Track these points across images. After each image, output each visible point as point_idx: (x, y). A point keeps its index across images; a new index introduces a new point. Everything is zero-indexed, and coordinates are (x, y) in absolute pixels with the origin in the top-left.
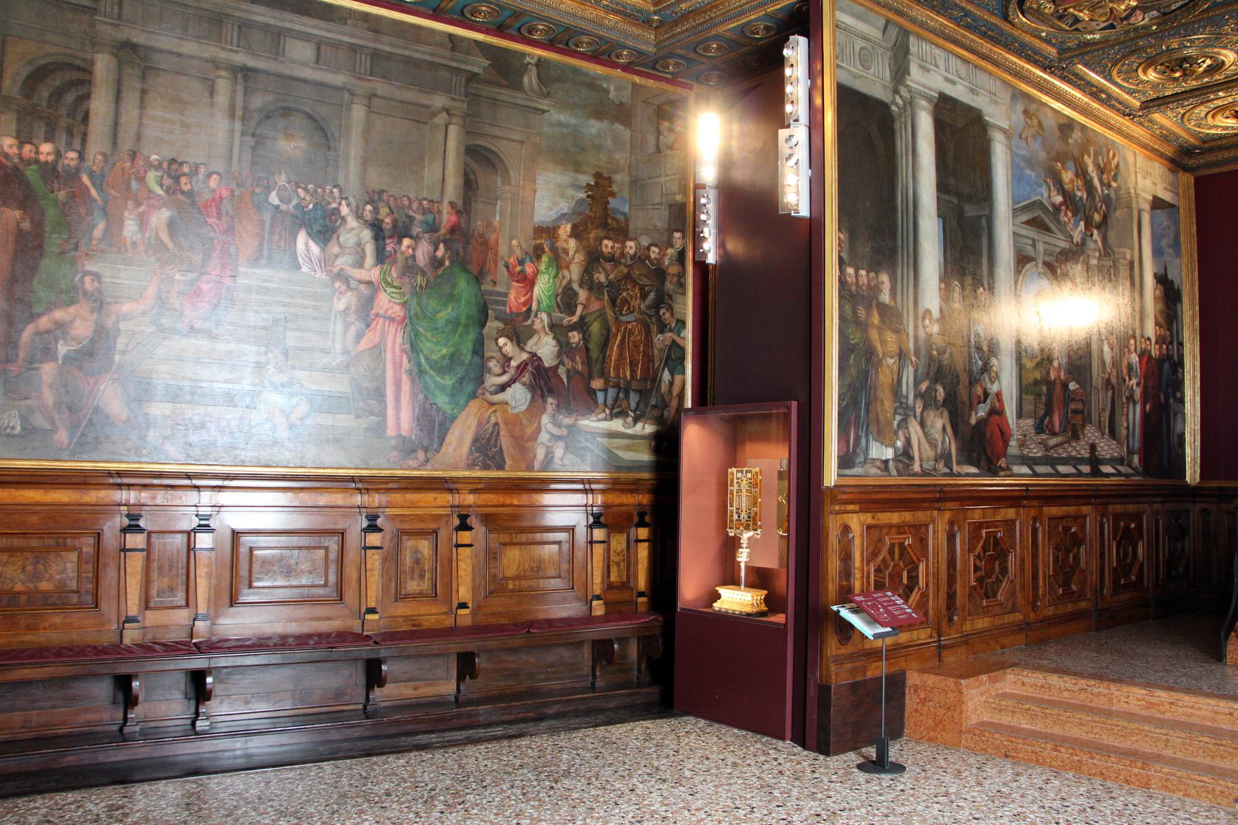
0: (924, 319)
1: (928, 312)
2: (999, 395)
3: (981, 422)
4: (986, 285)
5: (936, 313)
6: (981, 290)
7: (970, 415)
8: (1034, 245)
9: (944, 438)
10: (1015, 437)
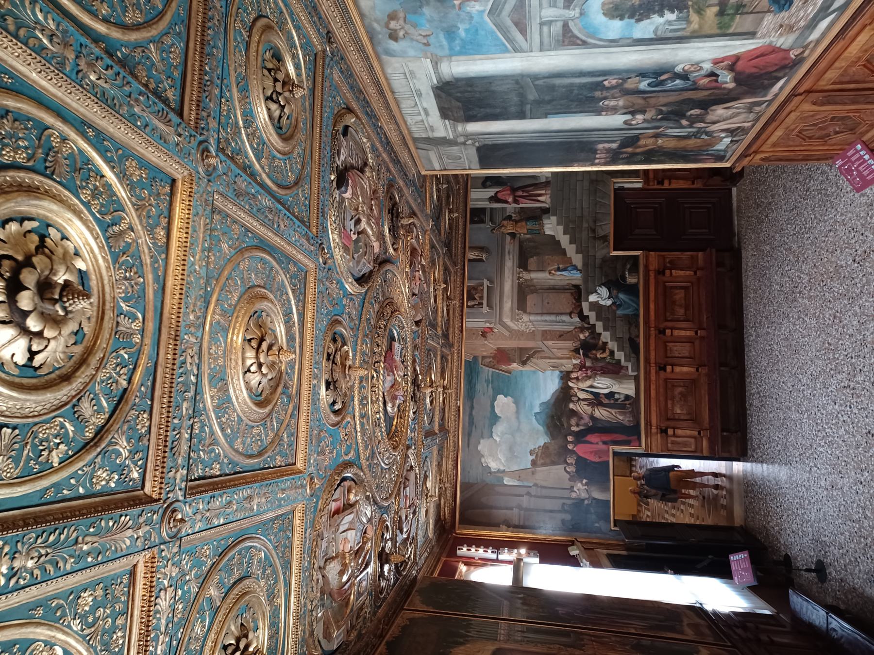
0: (631, 125)
1: (625, 122)
2: (716, 62)
3: (736, 80)
4: (600, 79)
5: (628, 117)
6: (606, 83)
7: (725, 88)
8: (550, 23)
9: (736, 108)
10: (774, 40)
